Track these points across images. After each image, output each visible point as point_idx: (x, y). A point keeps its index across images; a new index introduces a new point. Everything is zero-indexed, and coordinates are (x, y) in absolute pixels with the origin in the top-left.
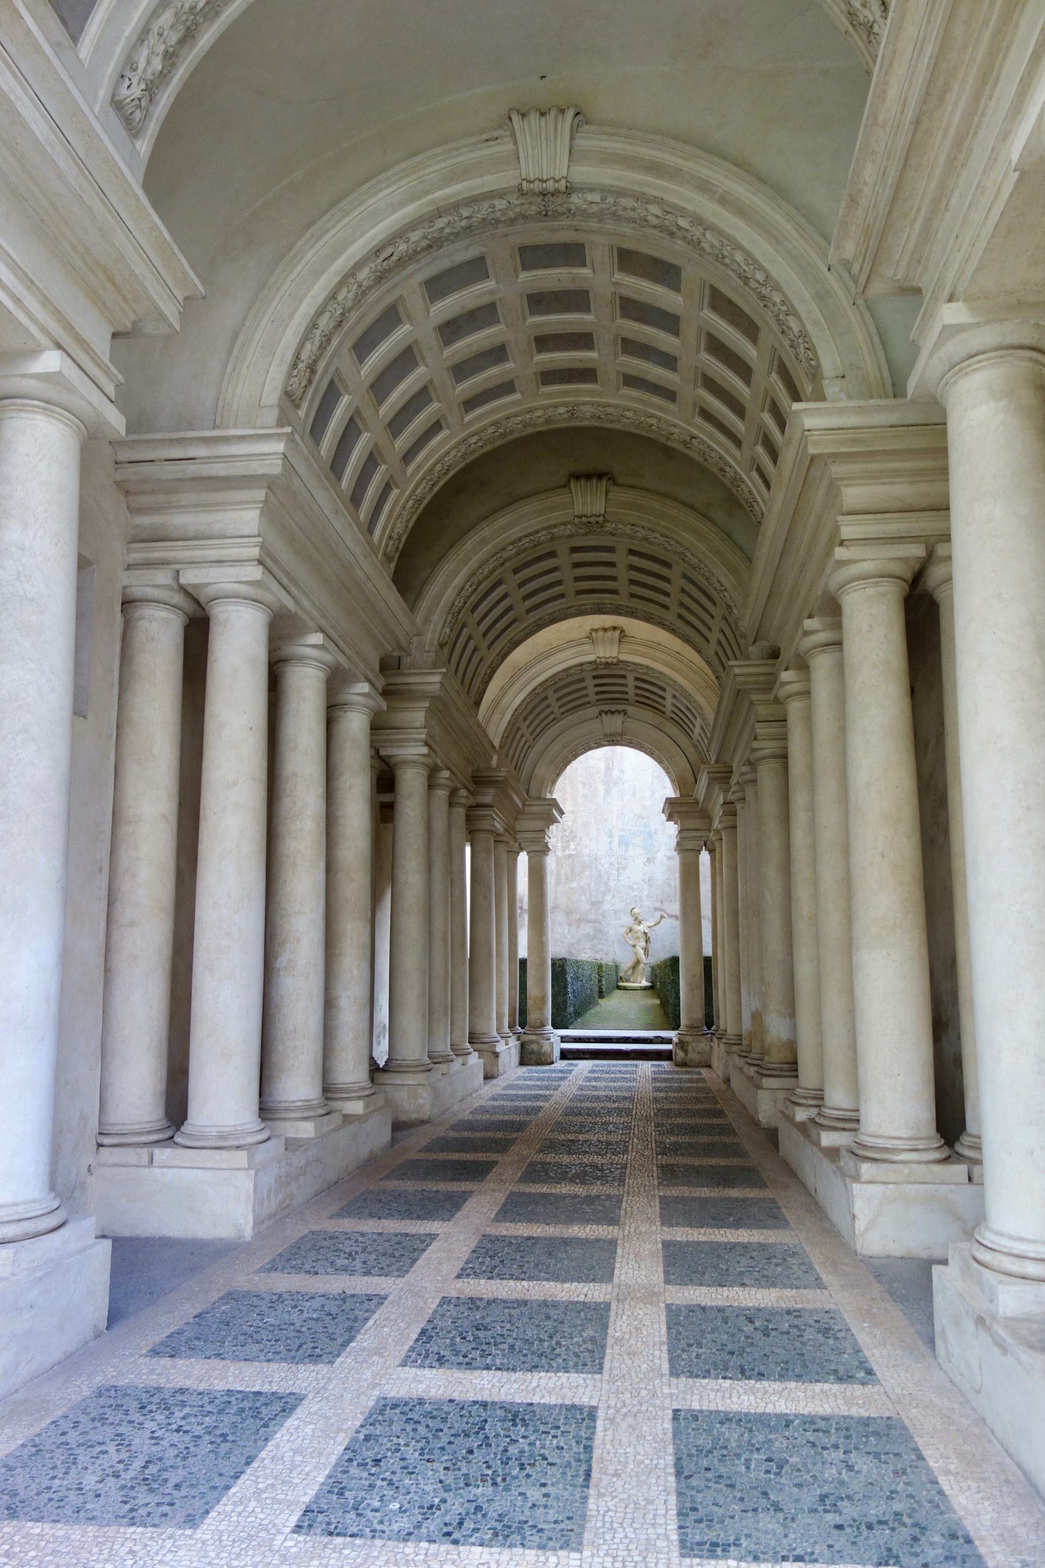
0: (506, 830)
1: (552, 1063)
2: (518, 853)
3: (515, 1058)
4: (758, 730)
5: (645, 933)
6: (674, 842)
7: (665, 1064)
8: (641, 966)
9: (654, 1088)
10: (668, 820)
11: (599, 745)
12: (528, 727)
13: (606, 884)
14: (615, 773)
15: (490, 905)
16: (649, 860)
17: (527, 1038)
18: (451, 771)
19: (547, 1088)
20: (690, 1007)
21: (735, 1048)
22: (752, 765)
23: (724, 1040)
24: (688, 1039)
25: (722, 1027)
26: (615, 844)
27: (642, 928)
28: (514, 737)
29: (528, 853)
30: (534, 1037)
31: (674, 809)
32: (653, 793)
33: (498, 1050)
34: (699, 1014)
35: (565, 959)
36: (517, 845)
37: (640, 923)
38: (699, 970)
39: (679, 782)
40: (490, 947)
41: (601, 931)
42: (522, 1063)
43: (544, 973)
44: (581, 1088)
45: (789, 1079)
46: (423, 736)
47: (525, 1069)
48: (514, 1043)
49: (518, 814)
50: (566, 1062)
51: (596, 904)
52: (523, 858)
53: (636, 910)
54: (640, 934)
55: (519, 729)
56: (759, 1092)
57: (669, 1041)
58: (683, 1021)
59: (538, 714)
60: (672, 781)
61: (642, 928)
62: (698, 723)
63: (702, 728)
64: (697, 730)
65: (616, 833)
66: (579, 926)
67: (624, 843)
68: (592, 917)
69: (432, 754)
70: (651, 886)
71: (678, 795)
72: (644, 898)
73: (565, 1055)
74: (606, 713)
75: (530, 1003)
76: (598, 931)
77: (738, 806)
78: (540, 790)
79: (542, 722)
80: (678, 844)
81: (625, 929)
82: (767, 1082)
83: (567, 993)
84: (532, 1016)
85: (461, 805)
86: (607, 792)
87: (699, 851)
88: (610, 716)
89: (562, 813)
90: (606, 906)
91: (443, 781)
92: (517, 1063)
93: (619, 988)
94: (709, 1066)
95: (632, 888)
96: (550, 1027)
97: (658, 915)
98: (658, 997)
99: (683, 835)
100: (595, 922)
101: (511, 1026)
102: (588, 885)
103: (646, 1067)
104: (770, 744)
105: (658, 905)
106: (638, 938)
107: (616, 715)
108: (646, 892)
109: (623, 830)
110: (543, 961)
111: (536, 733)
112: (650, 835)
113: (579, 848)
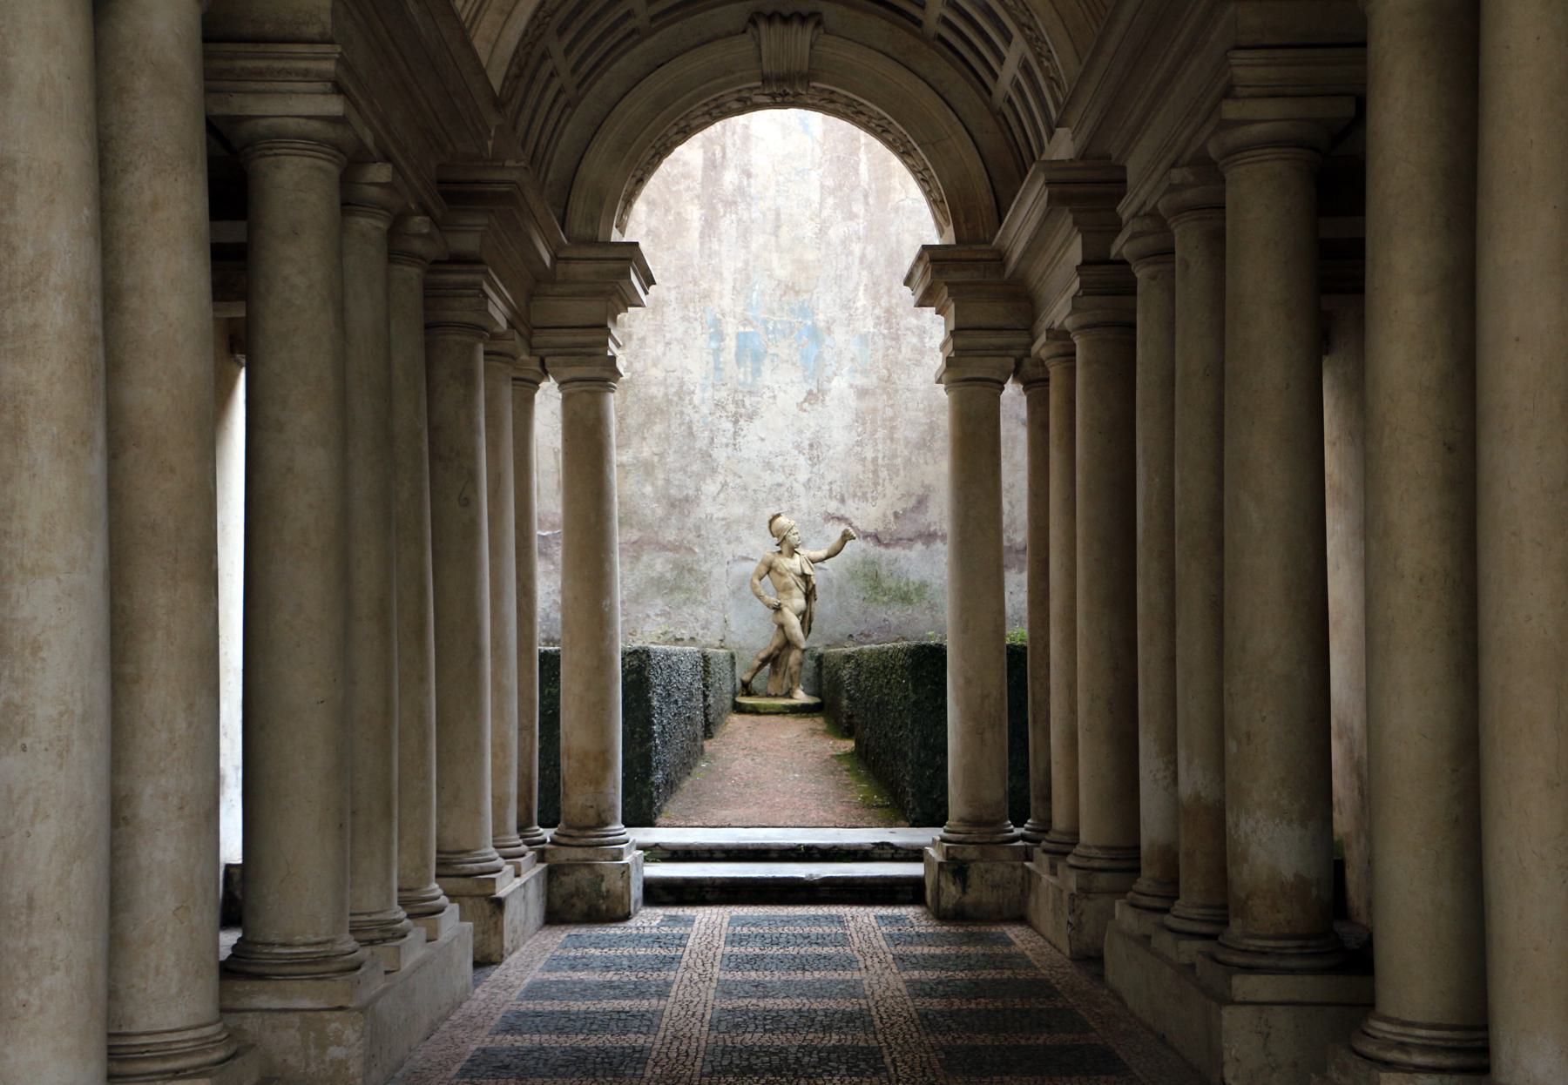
0: (511, 324)
1: (627, 917)
2: (535, 385)
3: (535, 912)
4: (1240, 72)
5: (805, 577)
6: (937, 361)
8: (794, 657)
9: (910, 983)
10: (921, 304)
11: (747, 105)
12: (567, 52)
13: (706, 456)
14: (730, 178)
15: (474, 523)
16: (811, 397)
17: (565, 855)
18: (397, 169)
19: (639, 991)
20: (972, 773)
21: (1102, 880)
22: (1209, 170)
23: (1071, 860)
24: (971, 852)
25: (1060, 820)
26: (729, 355)
27: (795, 563)
28: (533, 78)
29: (562, 384)
30: (579, 854)
31: (938, 275)
32: (822, 232)
33: (501, 893)
34: (995, 791)
35: (646, 652)
36: (535, 362)
37: (793, 551)
38: (997, 680)
39: (950, 201)
40: (477, 629)
41: (690, 570)
42: (554, 916)
43: (607, 690)
44: (726, 990)
45: (1289, 979)
46: (329, 66)
47: (561, 935)
48: (533, 871)
49: (536, 285)
50: (660, 911)
51: (679, 505)
52: (548, 403)
53: (783, 521)
54: (790, 579)
55: (545, 56)
56: (1227, 1012)
57: (914, 854)
59: (596, 17)
60: (934, 203)
61: (795, 563)
62: (1017, 51)
63: (1025, 68)
64: (1009, 70)
66: (637, 558)
68: (670, 535)
69: (354, 118)
70: (814, 461)
71: (950, 238)
72: (799, 489)
73: (658, 893)
74: (770, 19)
75: (567, 766)
76: (683, 569)
77: (1141, 273)
78: (593, 220)
79: (601, 39)
80: (950, 363)
81: (751, 567)
82: (1244, 985)
83: (651, 736)
84: (575, 800)
85: (413, 257)
86: (710, 226)
87: (1000, 386)
88: (778, 27)
89: (649, 280)
90: (708, 508)
91: (373, 192)
92: (539, 922)
93: (739, 709)
94: (1021, 919)
95: (768, 465)
96: (619, 826)
97: (835, 532)
98: (847, 733)
99: (961, 342)
100: (675, 548)
101: (523, 827)
102: (661, 455)
104: (1269, 109)
105: (833, 507)
106: (786, 589)
107: (796, 26)
108: (803, 476)
109: (746, 321)
110: (604, 661)
111: (584, 68)
112: (815, 334)
113: (638, 366)
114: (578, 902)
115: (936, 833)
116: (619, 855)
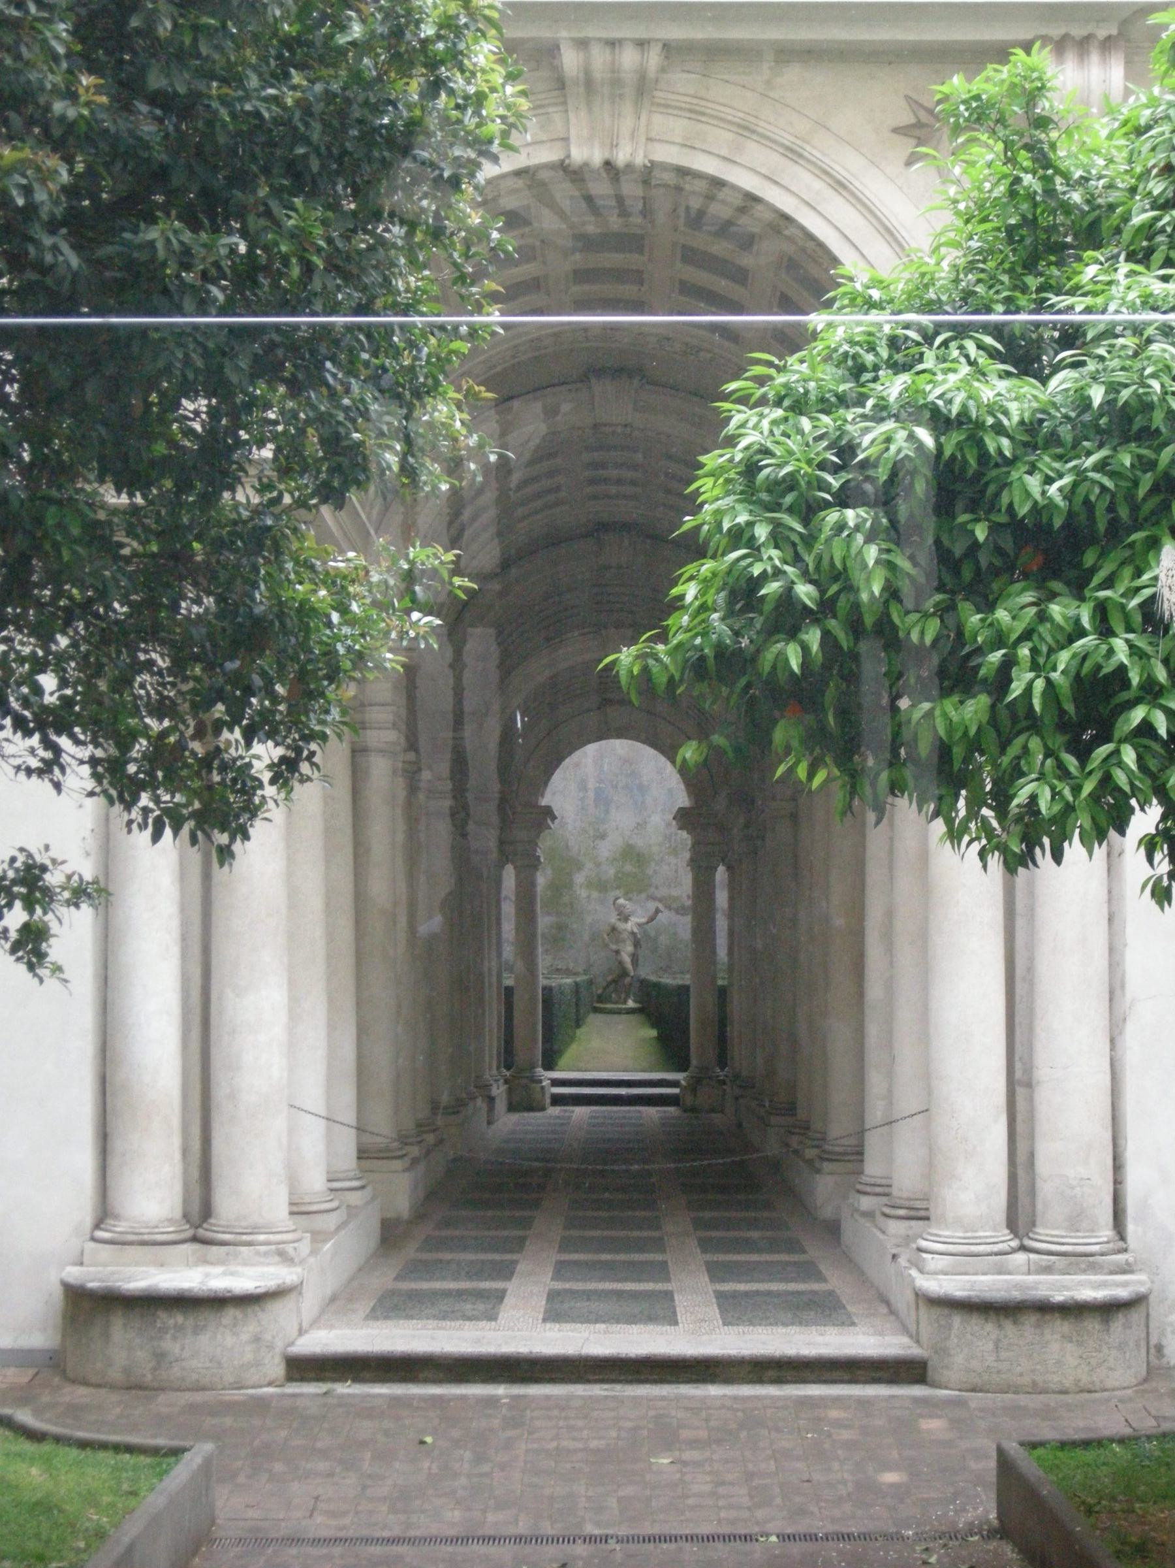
1: (543, 1109)
7: (671, 1109)
8: (627, 980)
27: (630, 926)
31: (684, 818)
37: (626, 919)
42: (512, 1108)
57: (675, 1084)
58: (694, 1062)
65: (592, 784)
67: (602, 800)
73: (557, 1100)
84: (521, 1057)
93: (596, 1010)
101: (498, 1068)
103: (652, 1112)
112: (642, 789)
114: (524, 1102)
115: (684, 1075)
116: (541, 1081)
